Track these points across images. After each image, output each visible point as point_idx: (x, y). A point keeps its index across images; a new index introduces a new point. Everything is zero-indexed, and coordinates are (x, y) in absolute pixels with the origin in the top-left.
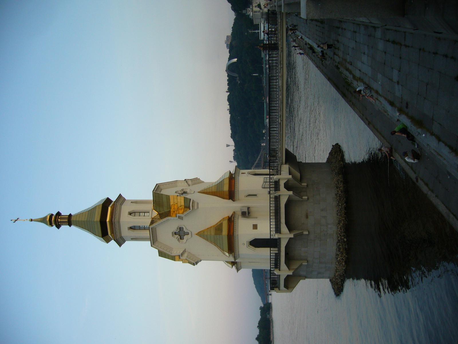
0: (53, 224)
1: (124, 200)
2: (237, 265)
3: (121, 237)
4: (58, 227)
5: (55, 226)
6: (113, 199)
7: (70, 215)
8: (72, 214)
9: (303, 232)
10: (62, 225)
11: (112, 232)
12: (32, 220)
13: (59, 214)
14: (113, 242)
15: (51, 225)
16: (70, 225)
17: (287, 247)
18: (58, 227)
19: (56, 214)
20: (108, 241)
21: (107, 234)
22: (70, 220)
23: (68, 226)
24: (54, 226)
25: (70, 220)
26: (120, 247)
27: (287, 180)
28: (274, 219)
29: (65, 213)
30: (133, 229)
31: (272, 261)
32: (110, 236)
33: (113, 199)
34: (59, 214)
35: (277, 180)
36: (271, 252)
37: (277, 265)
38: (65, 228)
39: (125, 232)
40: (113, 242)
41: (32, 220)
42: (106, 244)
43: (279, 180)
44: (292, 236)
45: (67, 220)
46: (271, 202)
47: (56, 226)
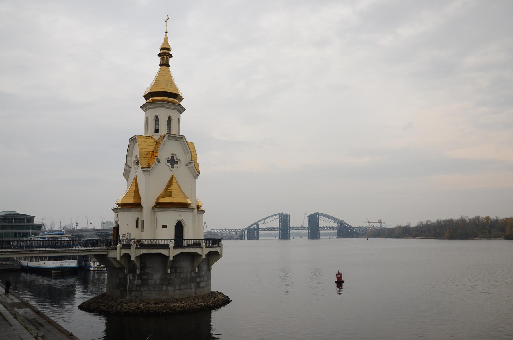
0: (162, 51)
1: (181, 113)
2: (120, 209)
4: (160, 55)
5: (160, 52)
6: (182, 103)
7: (169, 66)
8: (170, 67)
9: (138, 269)
10: (161, 58)
11: (154, 101)
12: (166, 33)
13: (171, 56)
14: (144, 101)
15: (162, 49)
16: (161, 65)
18: (160, 55)
19: (171, 54)
20: (146, 97)
21: (152, 97)
22: (165, 64)
23: (160, 64)
24: (160, 52)
25: (165, 64)
26: (140, 107)
27: (201, 254)
28: (151, 243)
29: (171, 61)
30: (156, 119)
31: (192, 241)
32: (151, 99)
33: (182, 103)
34: (171, 56)
35: (201, 246)
36: (190, 240)
38: (159, 60)
39: (153, 112)
40: (144, 101)
41: (166, 33)
42: (143, 94)
43: (202, 248)
45: (165, 63)
46: (195, 240)
47: (160, 53)
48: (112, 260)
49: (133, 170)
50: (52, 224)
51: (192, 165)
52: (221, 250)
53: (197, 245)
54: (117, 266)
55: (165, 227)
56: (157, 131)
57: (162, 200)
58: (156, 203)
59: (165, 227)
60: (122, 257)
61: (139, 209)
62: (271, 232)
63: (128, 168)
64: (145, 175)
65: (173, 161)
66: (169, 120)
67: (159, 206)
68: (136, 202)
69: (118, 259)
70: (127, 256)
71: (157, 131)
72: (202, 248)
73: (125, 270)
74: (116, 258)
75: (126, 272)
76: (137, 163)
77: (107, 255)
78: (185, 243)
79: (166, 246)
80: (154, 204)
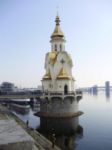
3: (53, 42)
4: (56, 21)
13: (60, 21)
14: (51, 39)
15: (56, 19)
16: (56, 25)
17: (59, 97)
18: (56, 21)
22: (58, 25)
24: (56, 20)
25: (58, 25)
29: (60, 23)
34: (60, 21)
37: (51, 94)
38: (55, 23)
39: (54, 43)
40: (51, 39)
42: (50, 37)
44: (63, 99)
48: (42, 100)
49: (48, 66)
50: (21, 87)
51: (70, 63)
52: (82, 95)
53: (73, 93)
54: (43, 101)
55: (60, 87)
56: (56, 50)
57: (59, 77)
58: (57, 78)
59: (60, 87)
60: (45, 98)
61: (51, 80)
62: (102, 88)
63: (46, 65)
64: (52, 67)
65: (63, 62)
66: (61, 46)
67: (58, 79)
68: (50, 78)
69: (43, 99)
70: (47, 98)
71: (56, 50)
72: (75, 95)
73: (46, 103)
74: (43, 99)
75: (46, 104)
76: (49, 63)
77: (39, 97)
78: (69, 93)
79: (61, 94)
80: (56, 78)
